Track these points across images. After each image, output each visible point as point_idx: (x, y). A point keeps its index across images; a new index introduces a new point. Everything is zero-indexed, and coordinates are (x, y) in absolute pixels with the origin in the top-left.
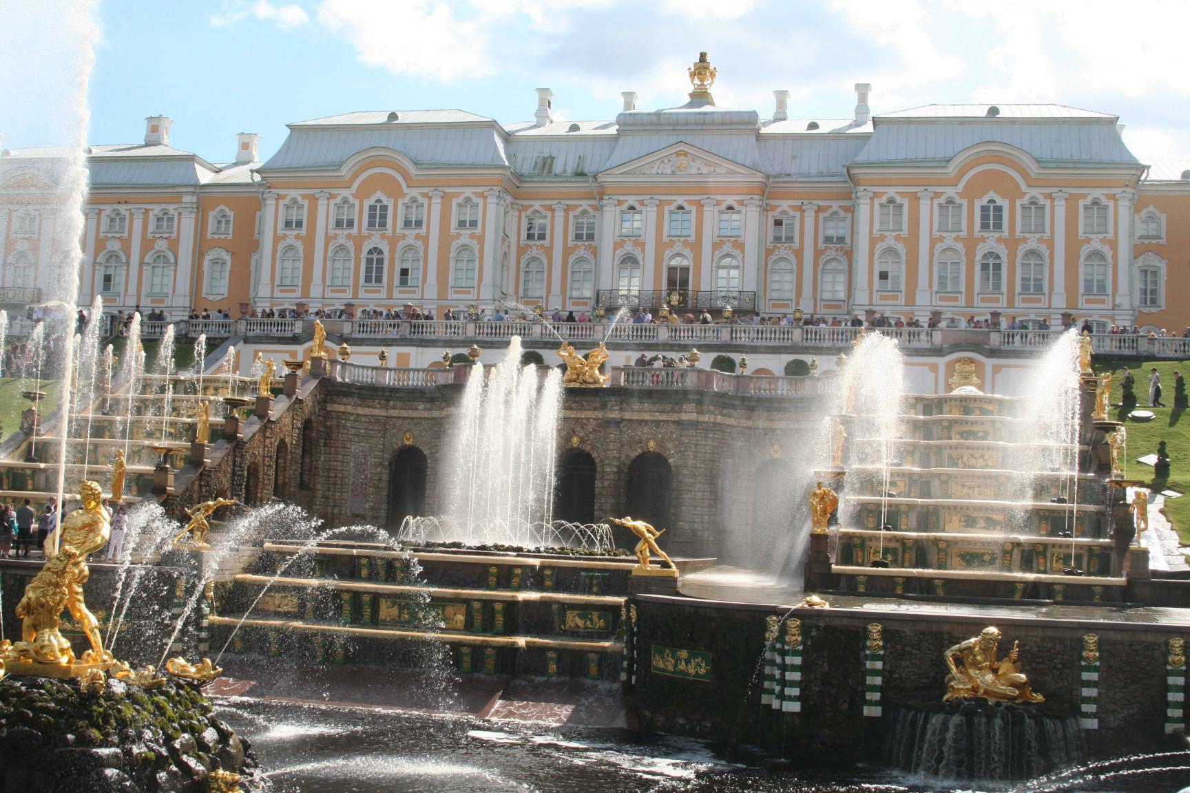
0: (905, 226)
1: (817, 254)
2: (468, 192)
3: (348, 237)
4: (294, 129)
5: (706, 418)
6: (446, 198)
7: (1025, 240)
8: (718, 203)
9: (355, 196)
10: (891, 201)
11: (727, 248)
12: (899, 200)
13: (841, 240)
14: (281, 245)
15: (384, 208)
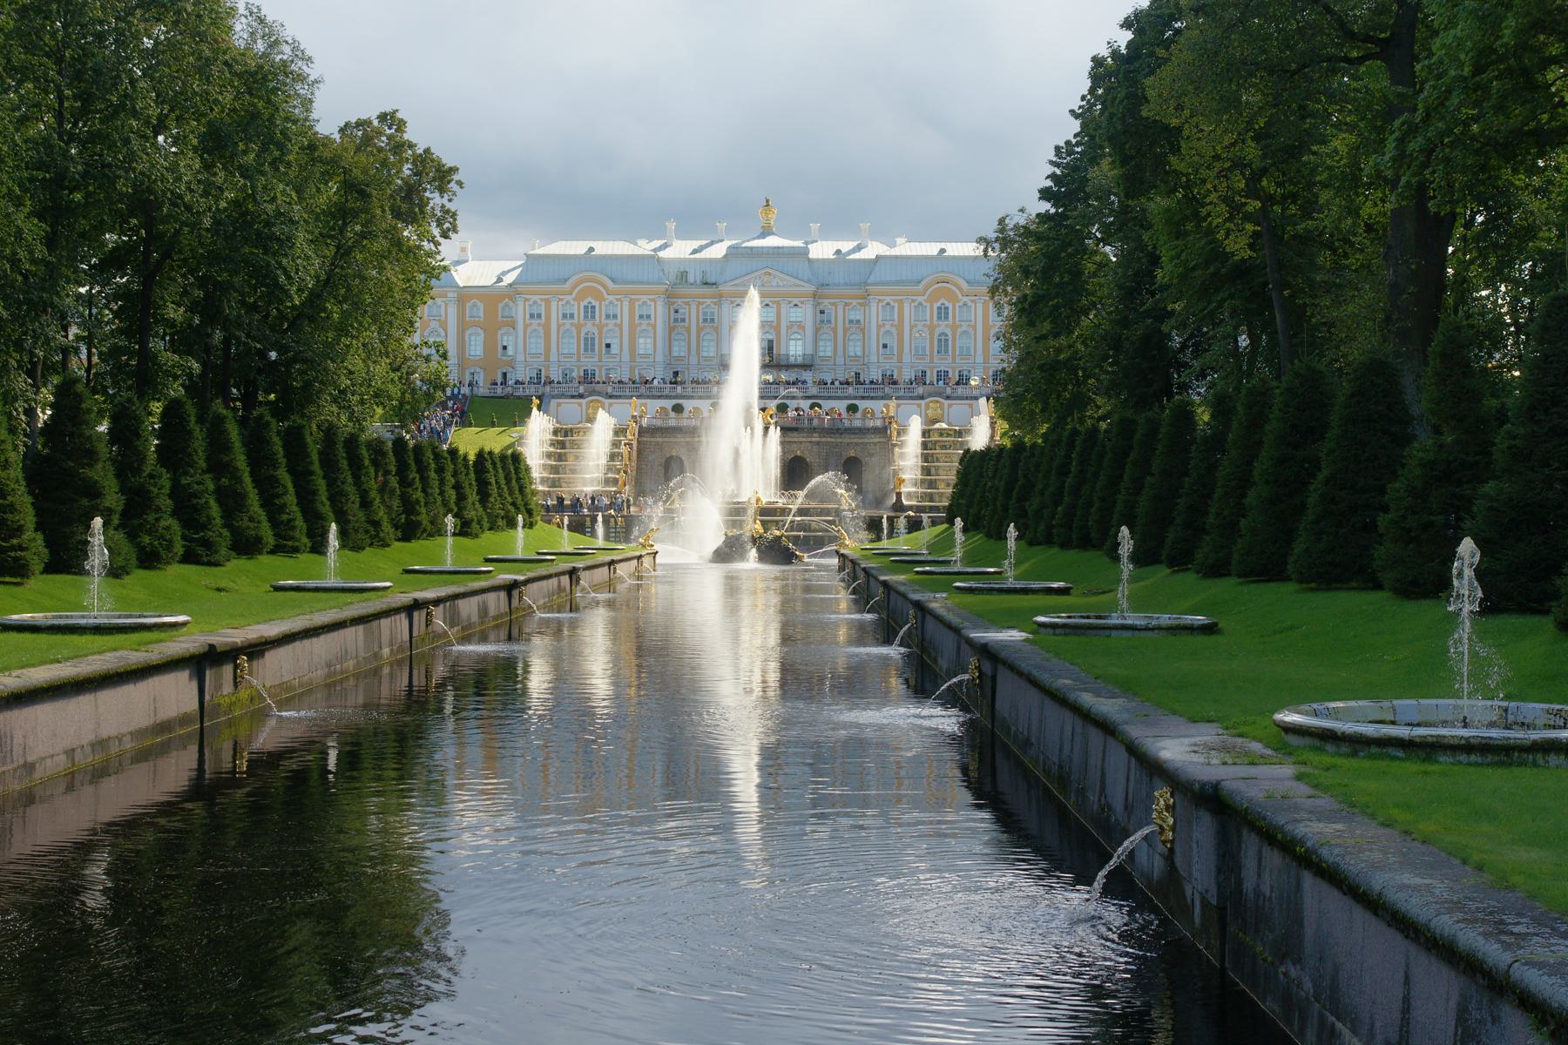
0: (896, 319)
1: (845, 330)
2: (644, 298)
3: (572, 324)
4: (527, 256)
5: (823, 440)
6: (632, 302)
7: (961, 326)
8: (790, 302)
9: (574, 300)
10: (888, 304)
11: (795, 329)
12: (892, 304)
13: (858, 321)
14: (529, 330)
15: (593, 307)
